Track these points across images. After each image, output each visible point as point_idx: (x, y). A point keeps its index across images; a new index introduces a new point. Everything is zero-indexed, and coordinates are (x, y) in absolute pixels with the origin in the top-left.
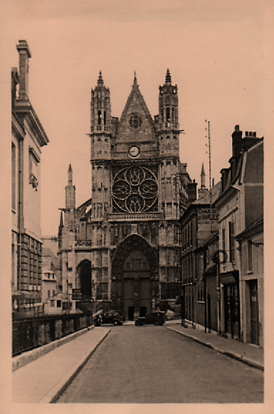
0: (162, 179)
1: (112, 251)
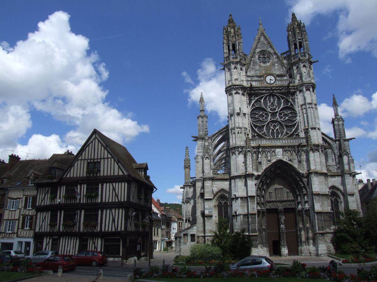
0: (301, 106)
1: (257, 178)
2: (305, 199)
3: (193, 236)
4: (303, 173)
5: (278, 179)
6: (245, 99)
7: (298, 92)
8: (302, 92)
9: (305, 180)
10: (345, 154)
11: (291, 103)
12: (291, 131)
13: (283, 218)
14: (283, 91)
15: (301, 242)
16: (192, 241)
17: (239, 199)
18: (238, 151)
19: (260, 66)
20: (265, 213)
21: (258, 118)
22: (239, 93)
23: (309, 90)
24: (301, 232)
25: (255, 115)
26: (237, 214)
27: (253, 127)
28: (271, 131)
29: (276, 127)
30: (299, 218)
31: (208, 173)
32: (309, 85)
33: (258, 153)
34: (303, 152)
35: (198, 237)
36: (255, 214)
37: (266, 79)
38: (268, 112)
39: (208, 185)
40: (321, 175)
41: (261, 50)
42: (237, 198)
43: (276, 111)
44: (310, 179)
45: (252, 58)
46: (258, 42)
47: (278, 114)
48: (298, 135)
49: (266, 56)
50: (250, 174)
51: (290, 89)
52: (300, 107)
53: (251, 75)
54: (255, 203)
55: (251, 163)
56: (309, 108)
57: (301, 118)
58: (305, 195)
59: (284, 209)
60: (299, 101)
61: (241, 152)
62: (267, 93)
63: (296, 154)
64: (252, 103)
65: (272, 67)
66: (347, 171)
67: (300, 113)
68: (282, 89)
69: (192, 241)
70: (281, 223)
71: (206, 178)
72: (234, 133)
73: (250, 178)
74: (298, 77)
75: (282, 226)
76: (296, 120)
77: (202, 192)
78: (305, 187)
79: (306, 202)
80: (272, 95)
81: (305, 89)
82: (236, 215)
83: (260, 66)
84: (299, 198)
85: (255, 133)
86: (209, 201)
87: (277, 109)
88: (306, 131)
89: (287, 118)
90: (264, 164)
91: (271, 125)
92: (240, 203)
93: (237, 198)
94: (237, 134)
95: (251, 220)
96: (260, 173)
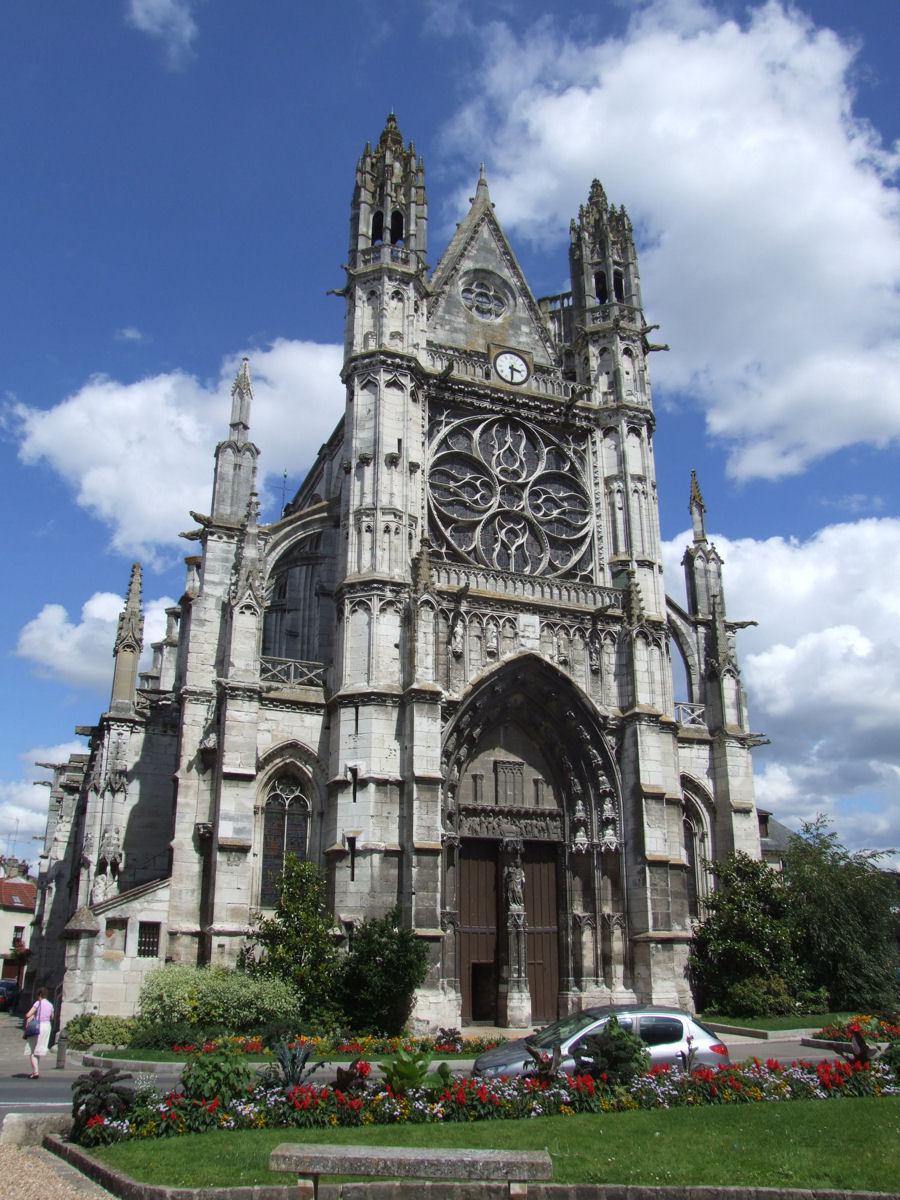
0: (608, 481)
1: (450, 708)
2: (602, 811)
3: (149, 930)
4: (605, 713)
6: (418, 413)
7: (598, 434)
8: (613, 434)
9: (610, 740)
10: (729, 671)
11: (572, 464)
12: (565, 561)
13: (520, 877)
14: (548, 418)
15: (578, 972)
16: (141, 953)
17: (372, 787)
18: (381, 600)
19: (470, 321)
20: (456, 853)
21: (455, 494)
22: (401, 387)
23: (638, 435)
24: (582, 933)
25: (444, 478)
26: (359, 845)
27: (438, 520)
28: (497, 550)
29: (517, 536)
30: (574, 883)
31: (244, 671)
32: (641, 416)
33: (455, 619)
34: (608, 641)
35: (173, 935)
36: (433, 852)
37: (499, 362)
38: (493, 480)
39: (240, 719)
40: (663, 728)
41: (478, 266)
42: (360, 784)
43: (520, 481)
44: (628, 742)
45: (446, 283)
46: (472, 238)
47: (526, 494)
48: (587, 579)
49: (492, 293)
50: (425, 692)
51: (575, 416)
52: (602, 486)
53: (435, 342)
54: (436, 807)
55: (431, 649)
56: (636, 491)
57: (605, 522)
58: (606, 794)
59: (526, 843)
60: (599, 464)
61: (390, 603)
62: (497, 413)
63: (586, 644)
64: (440, 436)
65: (510, 332)
66: (733, 727)
67: (602, 505)
68: (549, 410)
69: (141, 953)
70: (510, 895)
71: (237, 689)
72: (369, 529)
73: (426, 706)
74: (603, 384)
76: (585, 525)
77: (211, 742)
78: (607, 767)
79: (605, 824)
80: (509, 422)
81: (624, 427)
82: (352, 852)
83: (470, 321)
84: (581, 807)
85: (441, 547)
86: (242, 784)
87: (524, 475)
88: (621, 570)
89: (555, 513)
90: (473, 662)
91: (501, 527)
92: (372, 804)
93: (360, 784)
94: (380, 533)
95: (420, 874)
96: (457, 696)
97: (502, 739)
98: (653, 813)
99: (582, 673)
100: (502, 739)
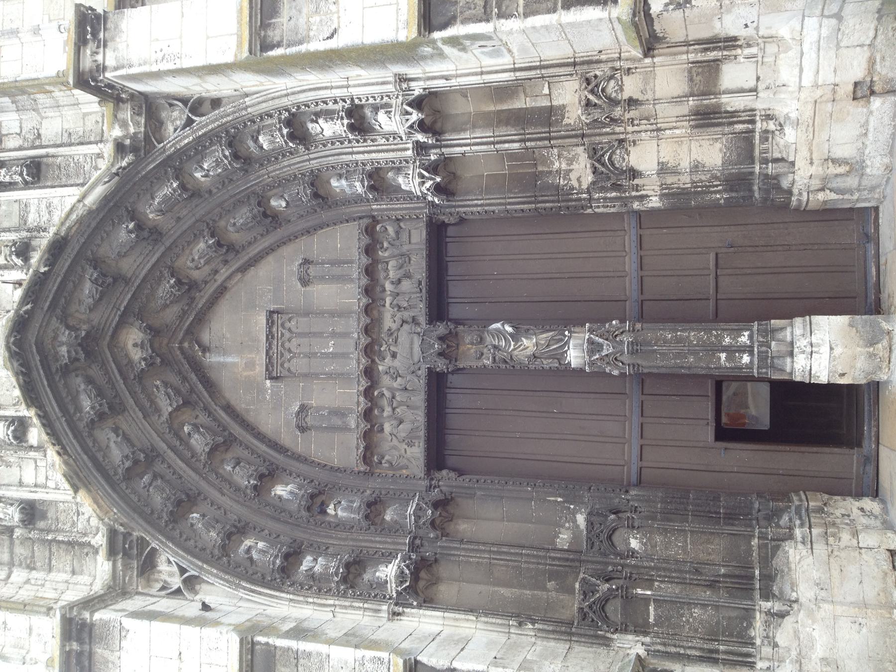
5: (205, 349)
70: (547, 363)
73: (99, 650)
75: (575, 356)
90: (41, 480)
97: (229, 359)
98: (302, 21)
99: (43, 206)
100: (229, 359)
